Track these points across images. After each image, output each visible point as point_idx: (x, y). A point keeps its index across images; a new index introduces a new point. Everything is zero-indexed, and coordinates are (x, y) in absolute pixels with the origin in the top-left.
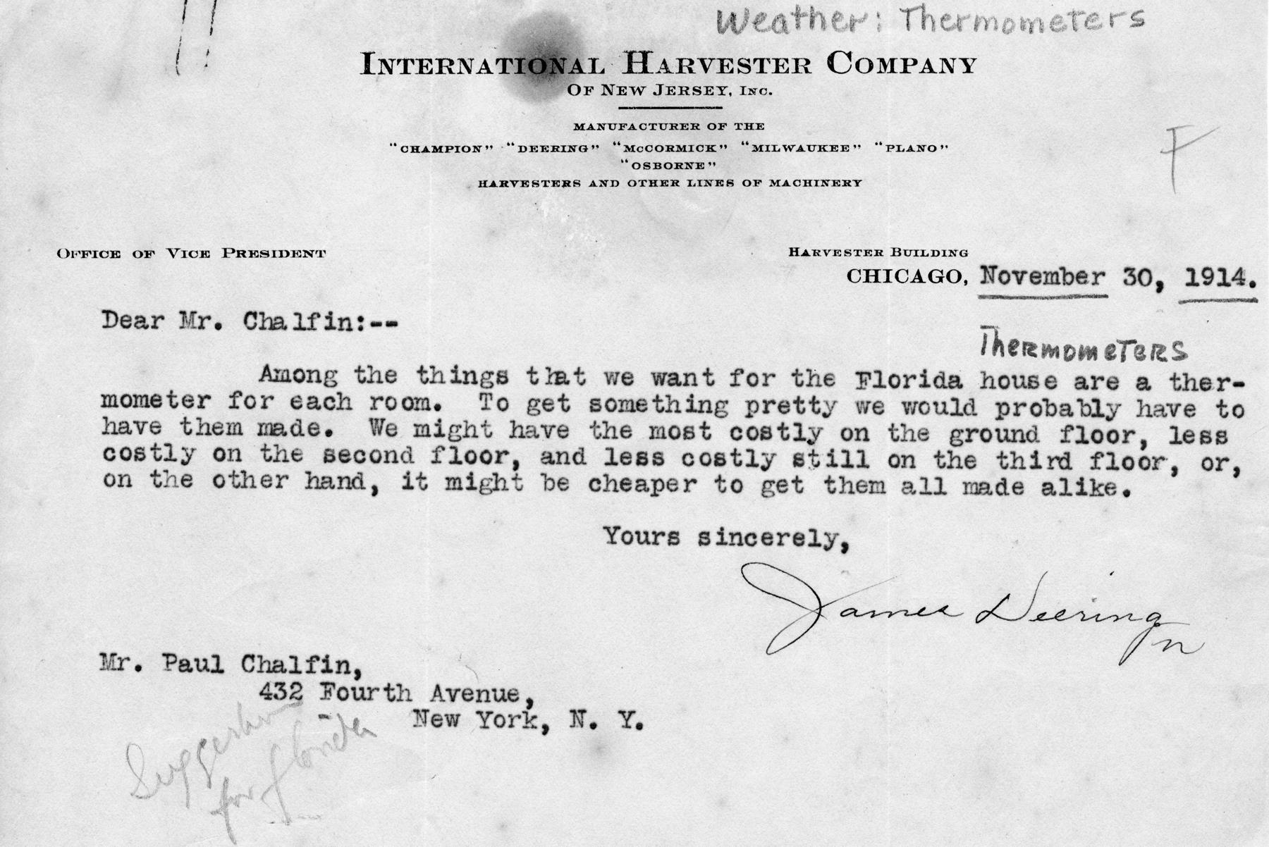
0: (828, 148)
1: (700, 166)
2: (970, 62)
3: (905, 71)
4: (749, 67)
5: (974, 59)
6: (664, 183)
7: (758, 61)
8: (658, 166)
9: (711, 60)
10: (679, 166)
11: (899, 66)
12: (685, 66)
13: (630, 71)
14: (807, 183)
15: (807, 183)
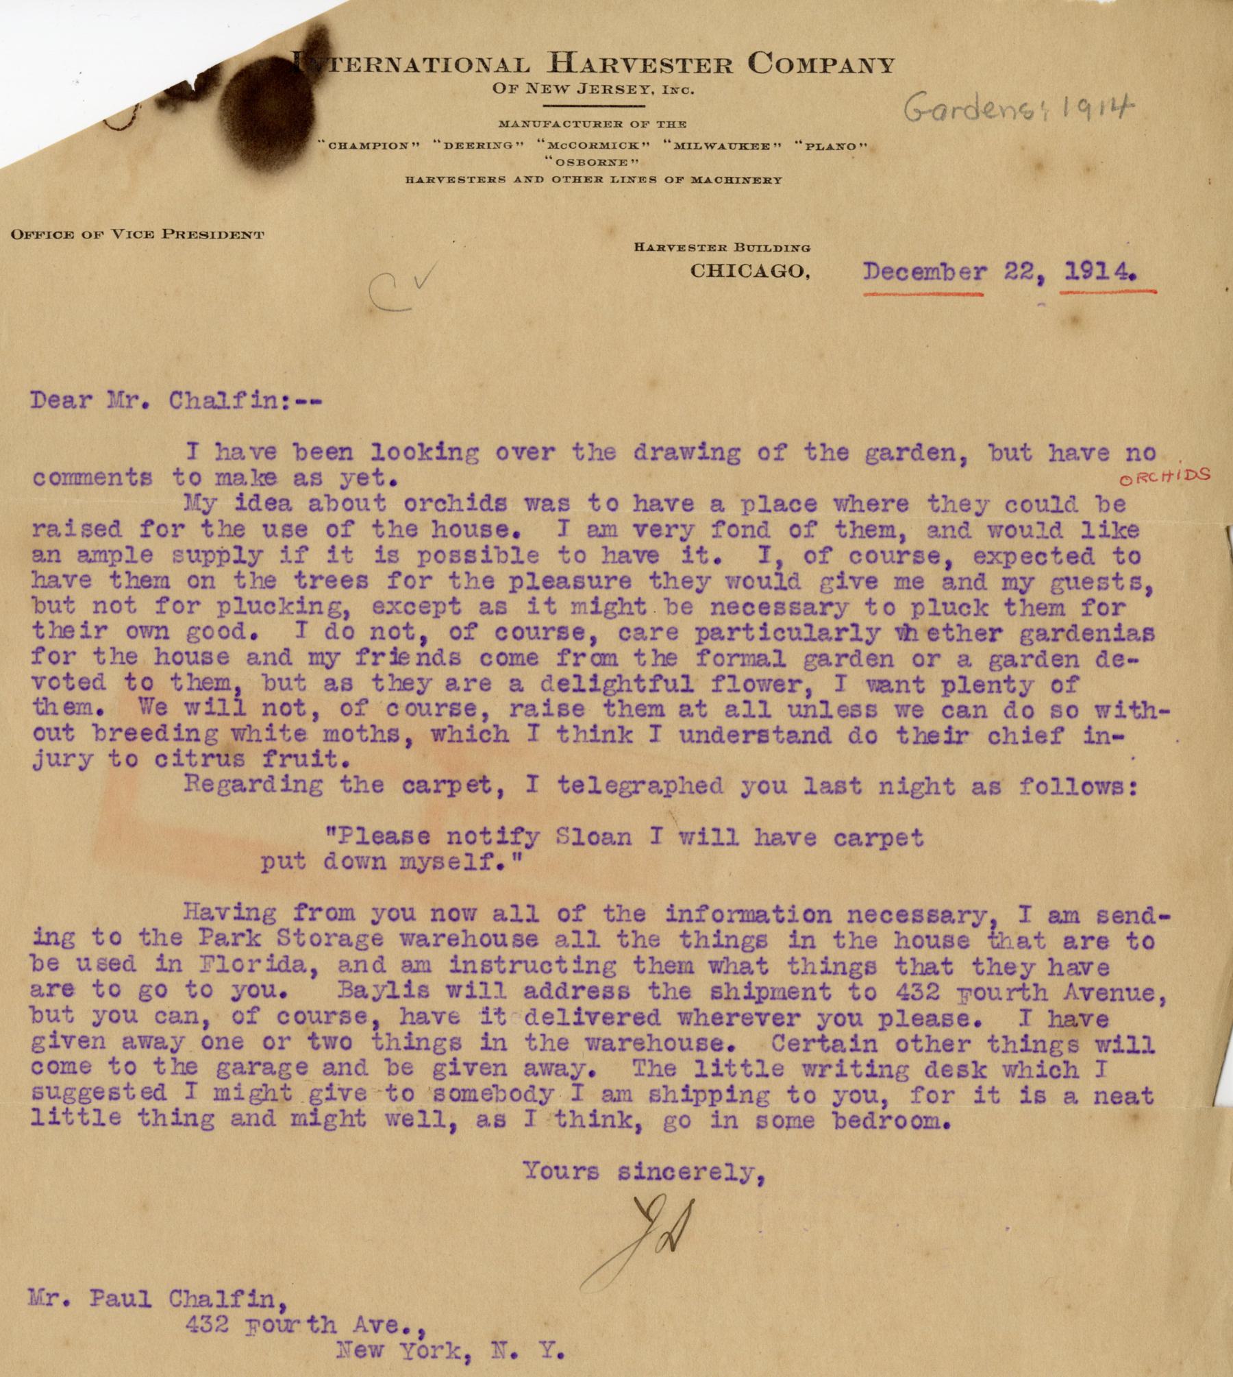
2: (888, 62)
4: (672, 68)
8: (581, 162)
10: (602, 163)
11: (819, 65)
13: (555, 70)
15: (729, 180)
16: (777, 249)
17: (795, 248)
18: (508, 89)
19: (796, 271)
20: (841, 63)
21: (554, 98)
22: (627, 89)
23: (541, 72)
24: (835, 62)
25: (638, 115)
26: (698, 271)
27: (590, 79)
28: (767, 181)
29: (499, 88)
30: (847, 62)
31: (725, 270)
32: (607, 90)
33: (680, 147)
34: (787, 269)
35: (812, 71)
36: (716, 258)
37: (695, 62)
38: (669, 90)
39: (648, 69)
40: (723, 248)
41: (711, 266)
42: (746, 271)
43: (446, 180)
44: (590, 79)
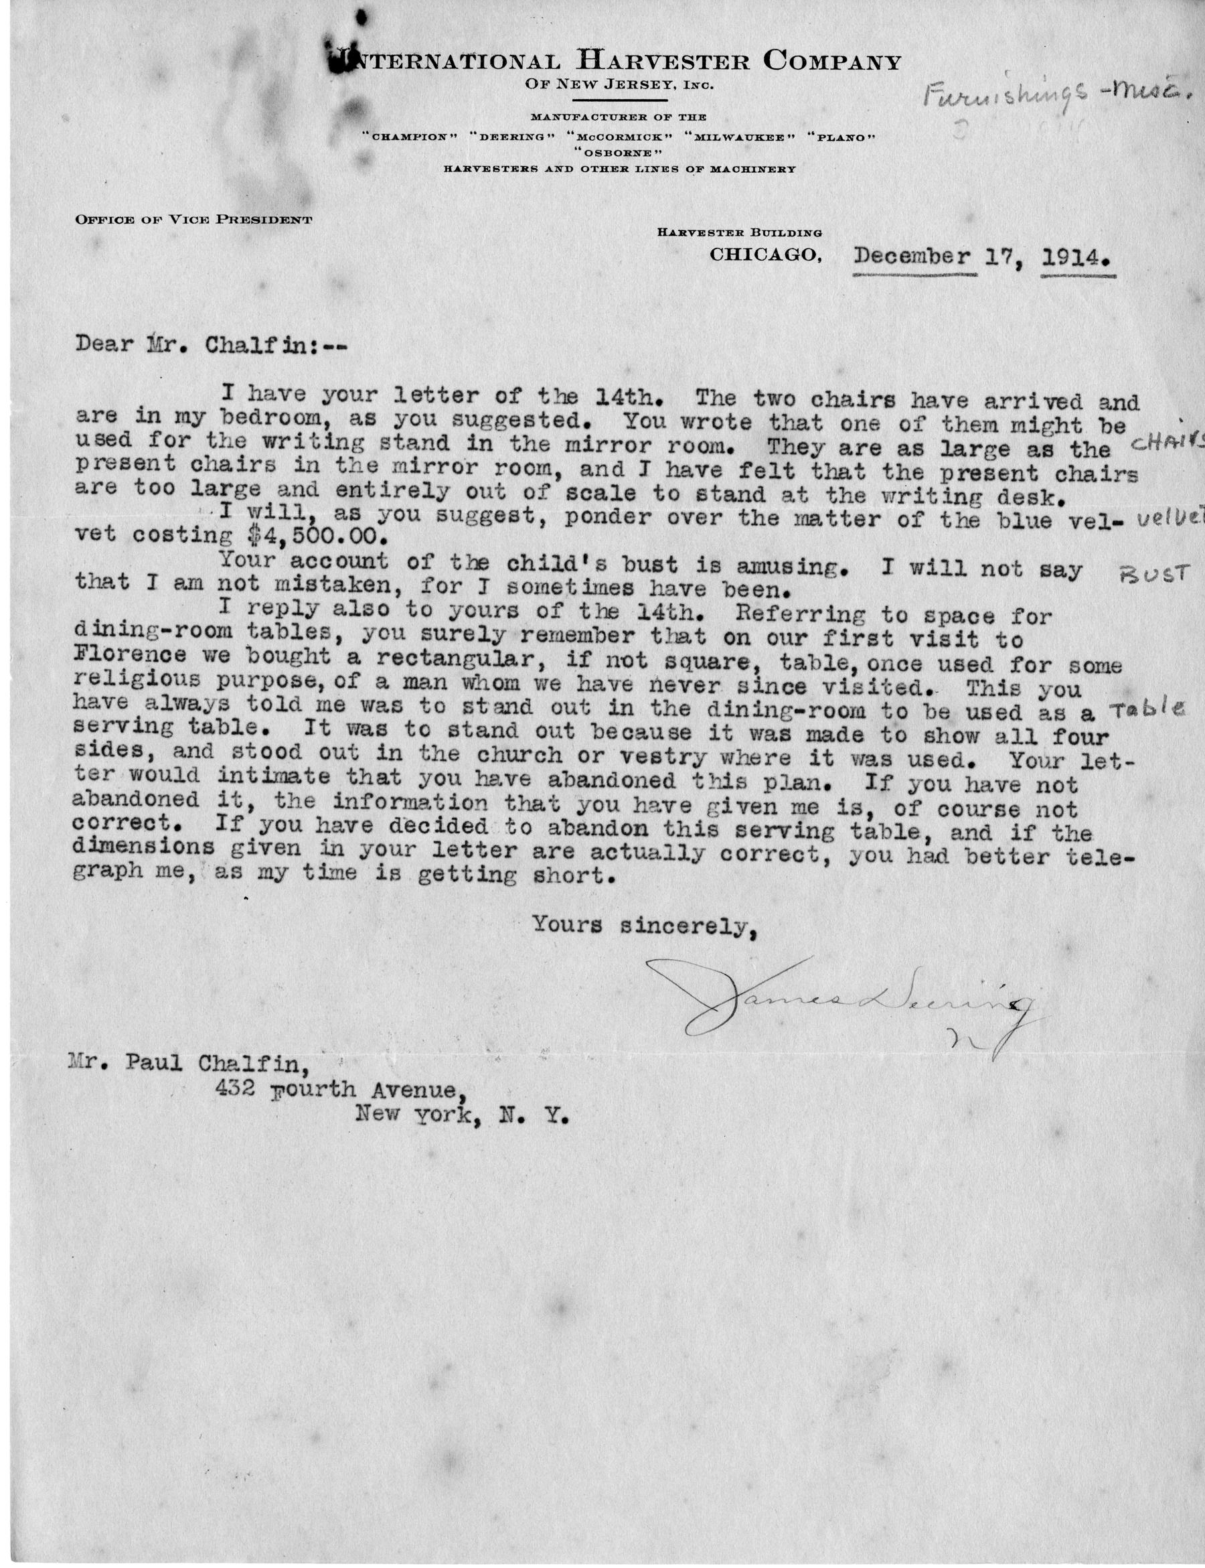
0: (765, 138)
1: (647, 153)
2: (895, 59)
3: (836, 68)
4: (692, 64)
5: (899, 57)
6: (614, 169)
7: (701, 59)
8: (608, 153)
9: (658, 56)
10: (628, 153)
11: (830, 62)
12: (634, 62)
13: (584, 66)
14: (746, 169)
15: (746, 169)
16: (791, 233)
17: (808, 233)
18: (540, 84)
19: (809, 255)
20: (851, 61)
21: (585, 93)
22: (651, 85)
23: (569, 66)
24: (845, 60)
25: (661, 108)
26: (717, 254)
27: (618, 75)
28: (782, 170)
29: (532, 83)
30: (857, 59)
31: (742, 254)
32: (632, 85)
33: (700, 138)
34: (800, 253)
35: (824, 67)
36: (733, 242)
37: (715, 59)
38: (690, 85)
39: (671, 65)
40: (740, 233)
41: (729, 250)
42: (761, 254)
43: (481, 169)
44: (618, 75)
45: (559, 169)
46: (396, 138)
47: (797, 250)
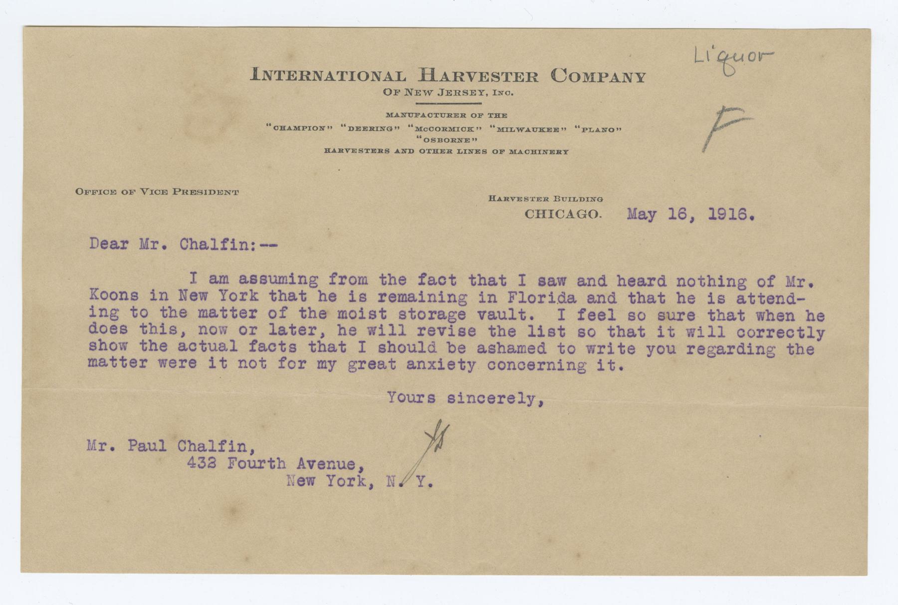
2: (641, 75)
3: (601, 81)
5: (644, 74)
11: (597, 78)
12: (458, 77)
21: (423, 98)
26: (530, 214)
31: (547, 214)
34: (587, 213)
36: (542, 206)
37: (514, 75)
41: (538, 211)
42: (560, 214)
45: (404, 151)
46: (290, 129)
47: (585, 211)
